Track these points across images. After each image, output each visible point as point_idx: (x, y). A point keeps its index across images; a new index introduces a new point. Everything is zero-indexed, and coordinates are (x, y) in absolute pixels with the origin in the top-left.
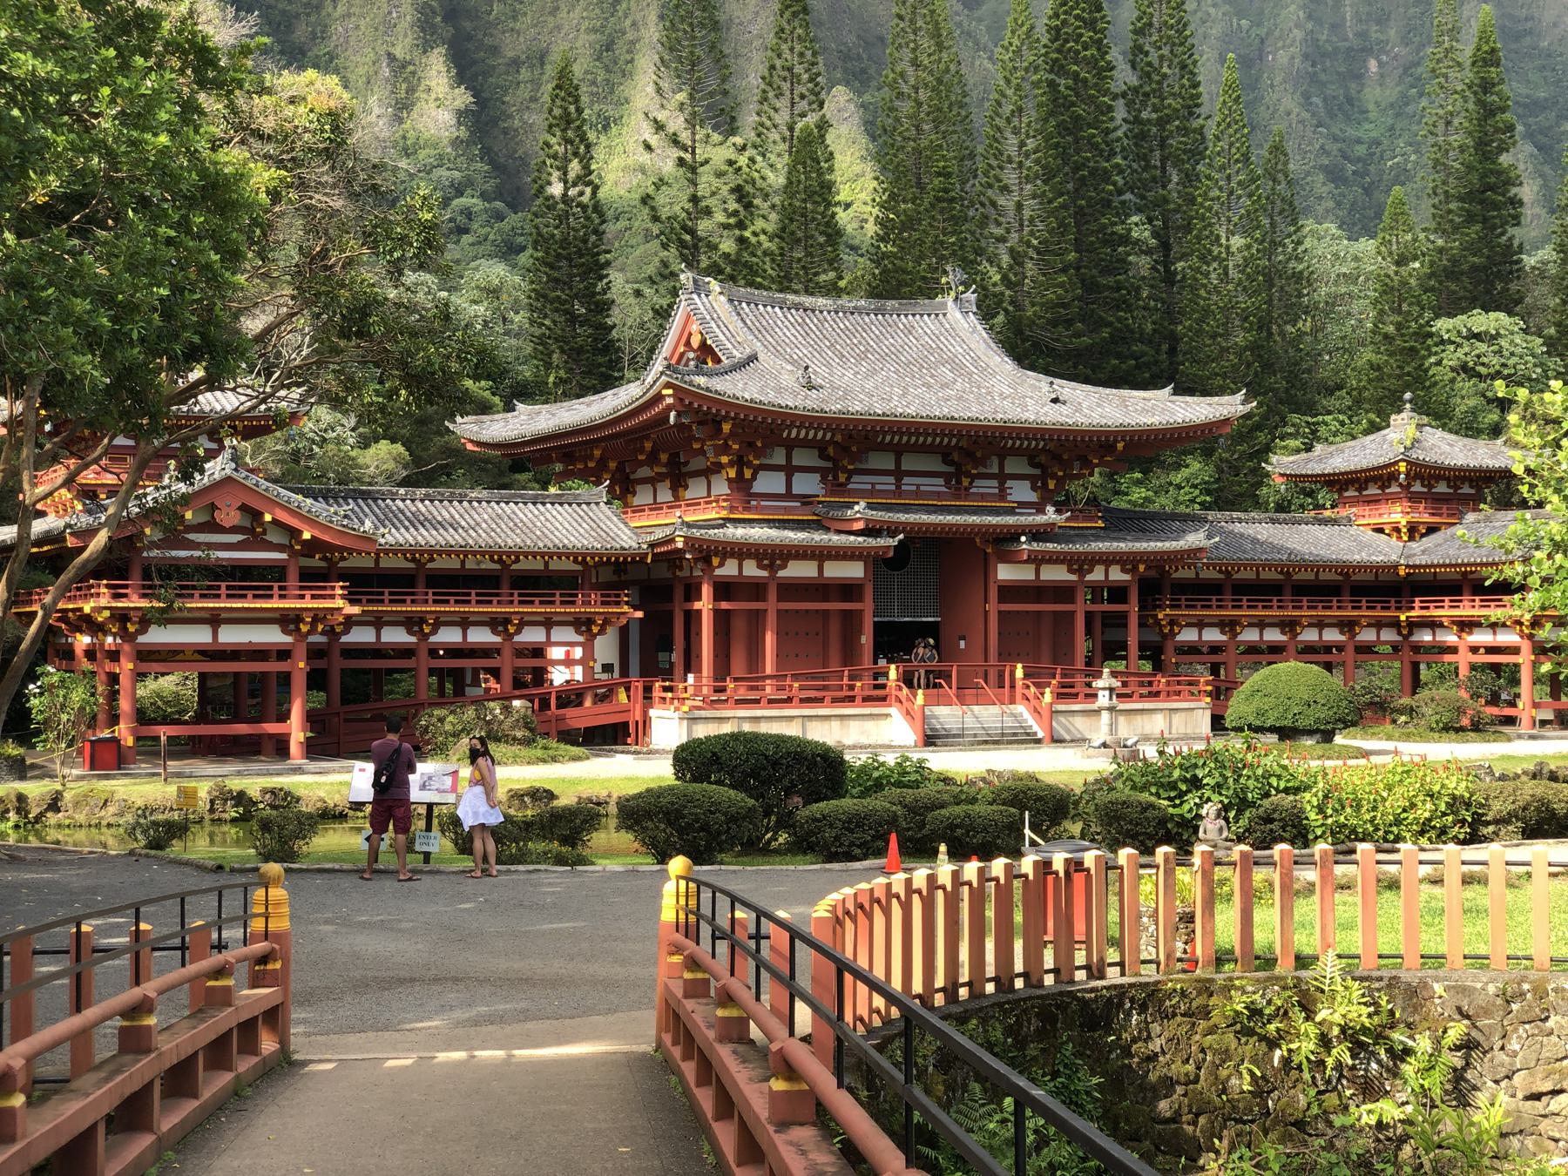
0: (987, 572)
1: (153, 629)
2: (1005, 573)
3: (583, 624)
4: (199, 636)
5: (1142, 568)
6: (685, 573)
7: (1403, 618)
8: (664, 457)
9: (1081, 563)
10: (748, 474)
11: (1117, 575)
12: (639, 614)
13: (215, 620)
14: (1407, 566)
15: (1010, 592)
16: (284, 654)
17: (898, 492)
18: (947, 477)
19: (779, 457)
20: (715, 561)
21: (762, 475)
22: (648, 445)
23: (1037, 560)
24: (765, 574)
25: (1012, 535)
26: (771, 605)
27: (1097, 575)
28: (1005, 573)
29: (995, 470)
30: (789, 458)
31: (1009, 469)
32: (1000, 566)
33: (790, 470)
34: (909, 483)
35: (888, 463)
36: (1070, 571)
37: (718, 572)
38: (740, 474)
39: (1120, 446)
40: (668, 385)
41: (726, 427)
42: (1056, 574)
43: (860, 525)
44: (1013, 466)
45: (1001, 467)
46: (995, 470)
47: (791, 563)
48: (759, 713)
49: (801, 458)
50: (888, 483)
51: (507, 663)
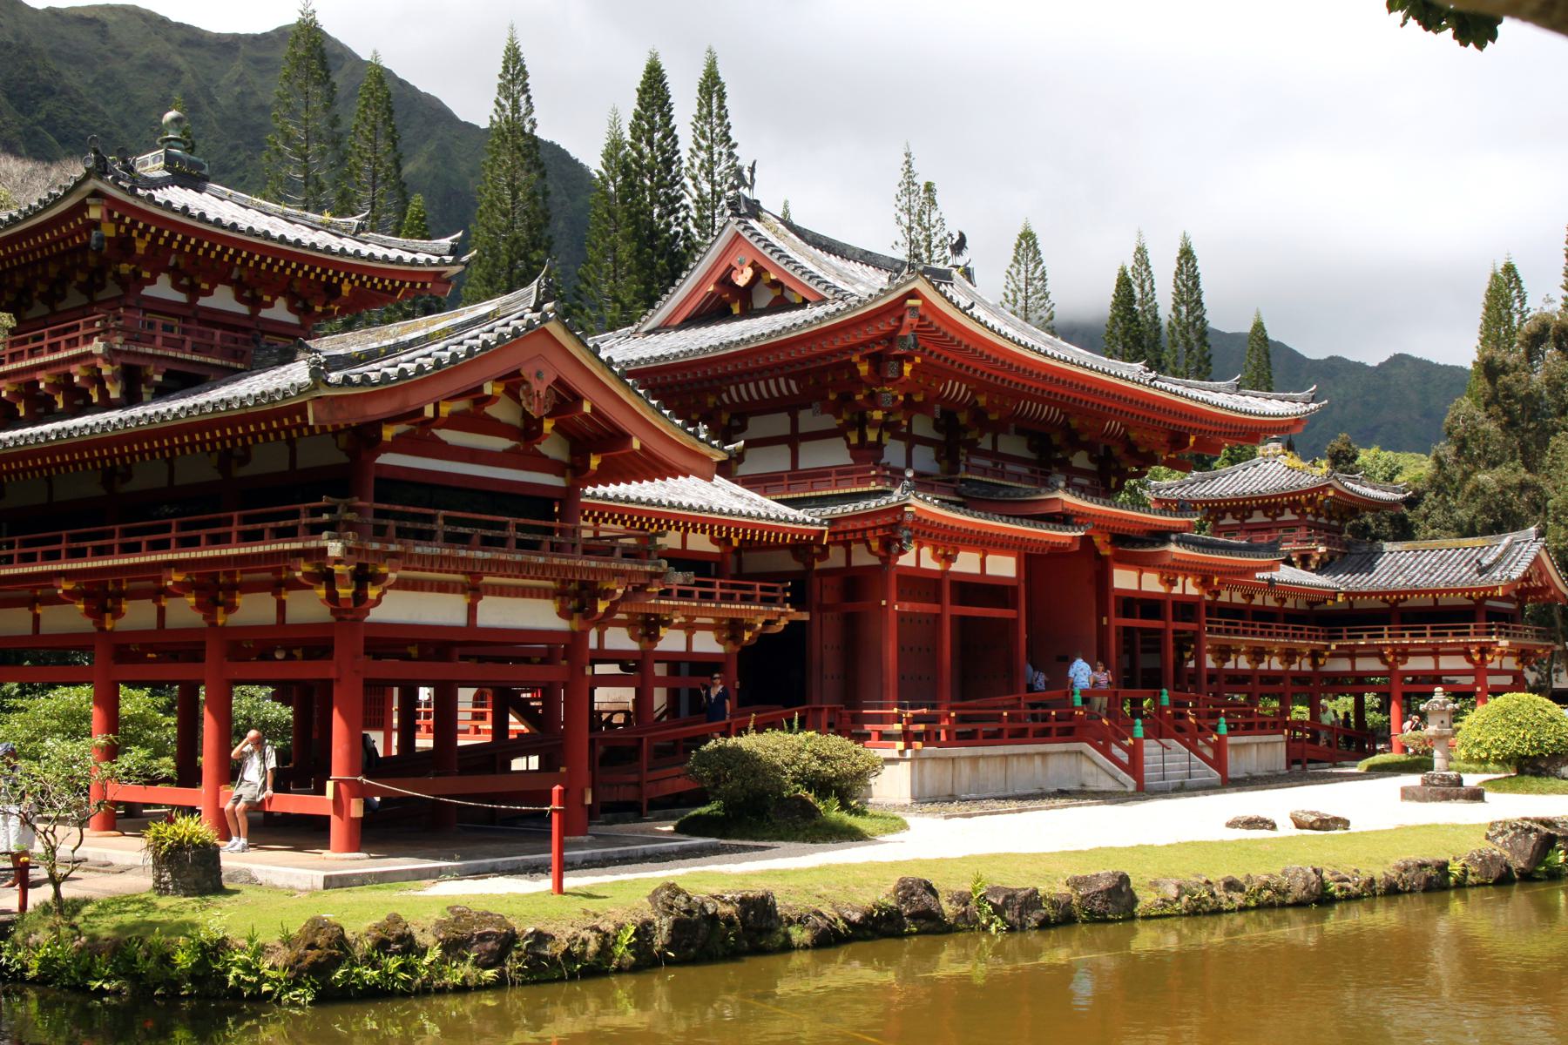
0: (1104, 578)
2: (1124, 579)
3: (731, 629)
5: (1216, 580)
6: (836, 558)
7: (1333, 647)
8: (725, 418)
9: (1170, 572)
10: (886, 436)
11: (1192, 590)
12: (805, 616)
14: (1347, 594)
22: (711, 400)
24: (936, 566)
25: (1161, 535)
26: (950, 610)
28: (1124, 579)
38: (880, 437)
39: (1192, 439)
40: (913, 294)
41: (907, 368)
42: (1152, 583)
43: (1058, 509)
48: (980, 750)
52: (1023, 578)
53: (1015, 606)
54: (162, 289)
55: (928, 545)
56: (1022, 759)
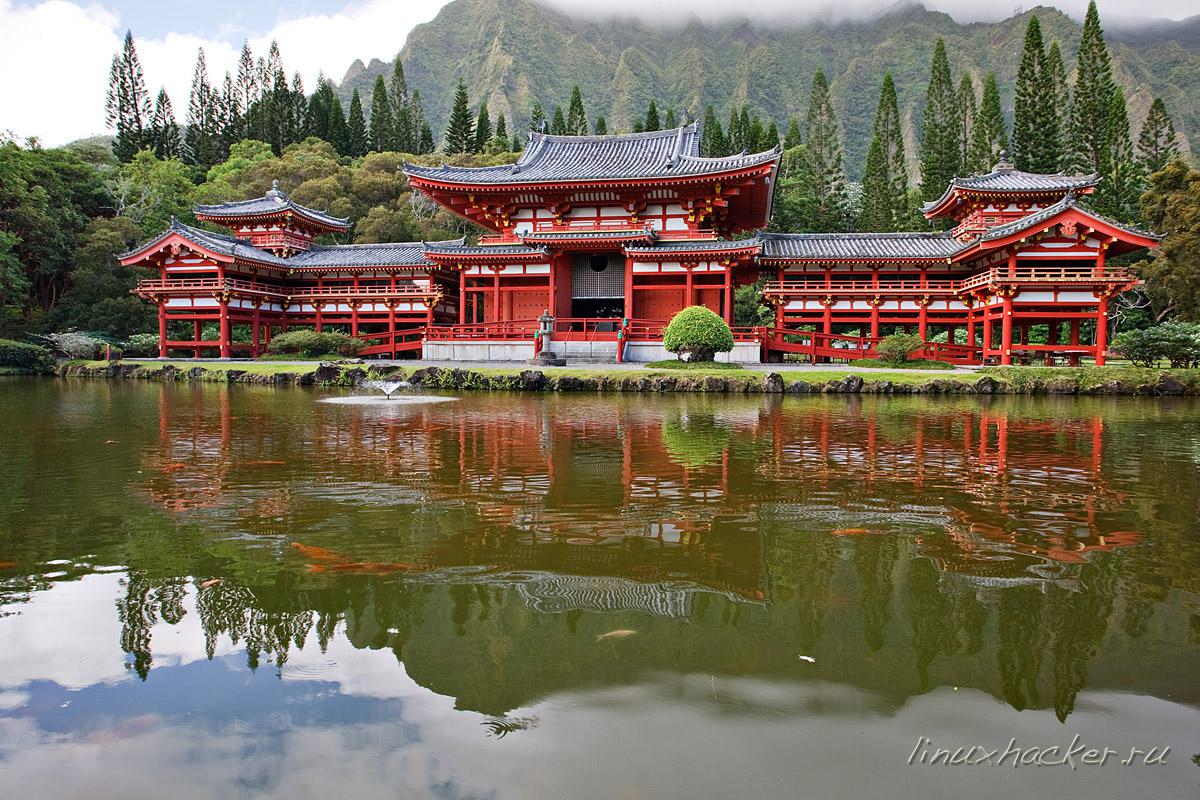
1: (171, 300)
4: (185, 303)
11: (715, 268)
13: (192, 296)
15: (639, 279)
16: (216, 311)
18: (628, 218)
20: (460, 267)
21: (519, 224)
27: (702, 268)
30: (535, 215)
31: (668, 213)
33: (535, 220)
35: (593, 213)
36: (682, 265)
37: (467, 272)
39: (718, 190)
41: (472, 199)
47: (507, 267)
48: (465, 342)
49: (541, 214)
53: (548, 284)
55: (485, 264)
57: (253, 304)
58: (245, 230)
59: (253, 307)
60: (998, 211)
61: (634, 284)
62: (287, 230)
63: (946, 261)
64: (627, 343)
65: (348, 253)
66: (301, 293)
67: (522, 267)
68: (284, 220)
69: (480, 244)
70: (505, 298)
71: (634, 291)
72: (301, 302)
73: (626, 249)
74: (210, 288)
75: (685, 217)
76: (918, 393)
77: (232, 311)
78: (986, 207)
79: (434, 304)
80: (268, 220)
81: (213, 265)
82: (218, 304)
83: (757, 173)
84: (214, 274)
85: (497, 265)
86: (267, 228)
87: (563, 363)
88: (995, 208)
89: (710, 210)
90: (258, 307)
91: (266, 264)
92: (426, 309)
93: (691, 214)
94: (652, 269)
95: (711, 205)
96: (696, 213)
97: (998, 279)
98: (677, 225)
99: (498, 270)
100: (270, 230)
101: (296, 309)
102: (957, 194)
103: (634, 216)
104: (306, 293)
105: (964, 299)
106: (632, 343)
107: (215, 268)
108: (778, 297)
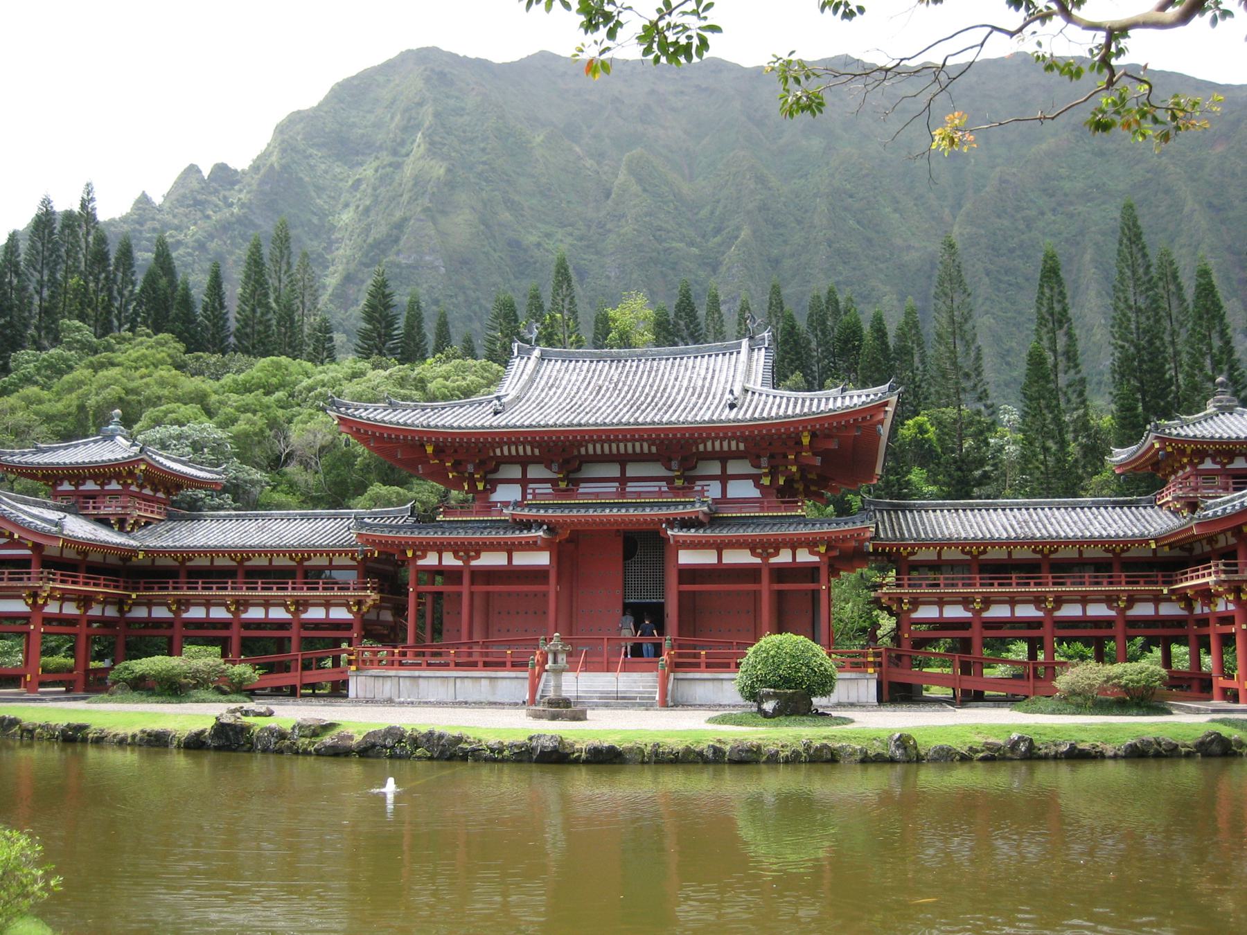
7: (1165, 591)
11: (804, 556)
14: (1156, 540)
17: (622, 493)
19: (516, 473)
20: (410, 554)
23: (720, 547)
27: (784, 557)
29: (719, 473)
31: (730, 471)
32: (681, 552)
33: (524, 482)
34: (631, 487)
35: (614, 471)
36: (754, 554)
37: (420, 562)
39: (806, 441)
41: (430, 449)
42: (742, 557)
44: (734, 468)
45: (724, 469)
46: (719, 473)
47: (483, 555)
48: (417, 673)
49: (534, 472)
50: (612, 487)
51: (294, 633)
52: (554, 565)
54: (66, 486)
56: (466, 680)
57: (78, 608)
58: (66, 486)
59: (77, 612)
60: (1218, 467)
61: (680, 582)
62: (134, 488)
63: (1148, 544)
64: (672, 675)
65: (228, 524)
66: (152, 589)
67: (505, 555)
68: (131, 474)
69: (440, 518)
70: (478, 602)
71: (680, 593)
72: (150, 604)
73: (669, 532)
74: (19, 584)
75: (756, 479)
76: (1115, 757)
77: (48, 620)
78: (1202, 462)
79: (364, 609)
80: (102, 473)
81: (25, 547)
82: (28, 609)
83: (864, 419)
84: (23, 563)
85: (467, 553)
86: (102, 485)
87: (579, 716)
88: (1214, 462)
89: (794, 469)
90: (86, 611)
91: (105, 547)
92: (350, 616)
93: (766, 475)
94: (707, 558)
95: (796, 462)
96: (773, 474)
97: (1223, 577)
98: (743, 490)
99: (470, 558)
100: (107, 487)
101: (141, 613)
102: (1157, 446)
103: (678, 477)
104: (160, 589)
105: (1179, 600)
106: (680, 675)
107: (28, 552)
108: (900, 601)
